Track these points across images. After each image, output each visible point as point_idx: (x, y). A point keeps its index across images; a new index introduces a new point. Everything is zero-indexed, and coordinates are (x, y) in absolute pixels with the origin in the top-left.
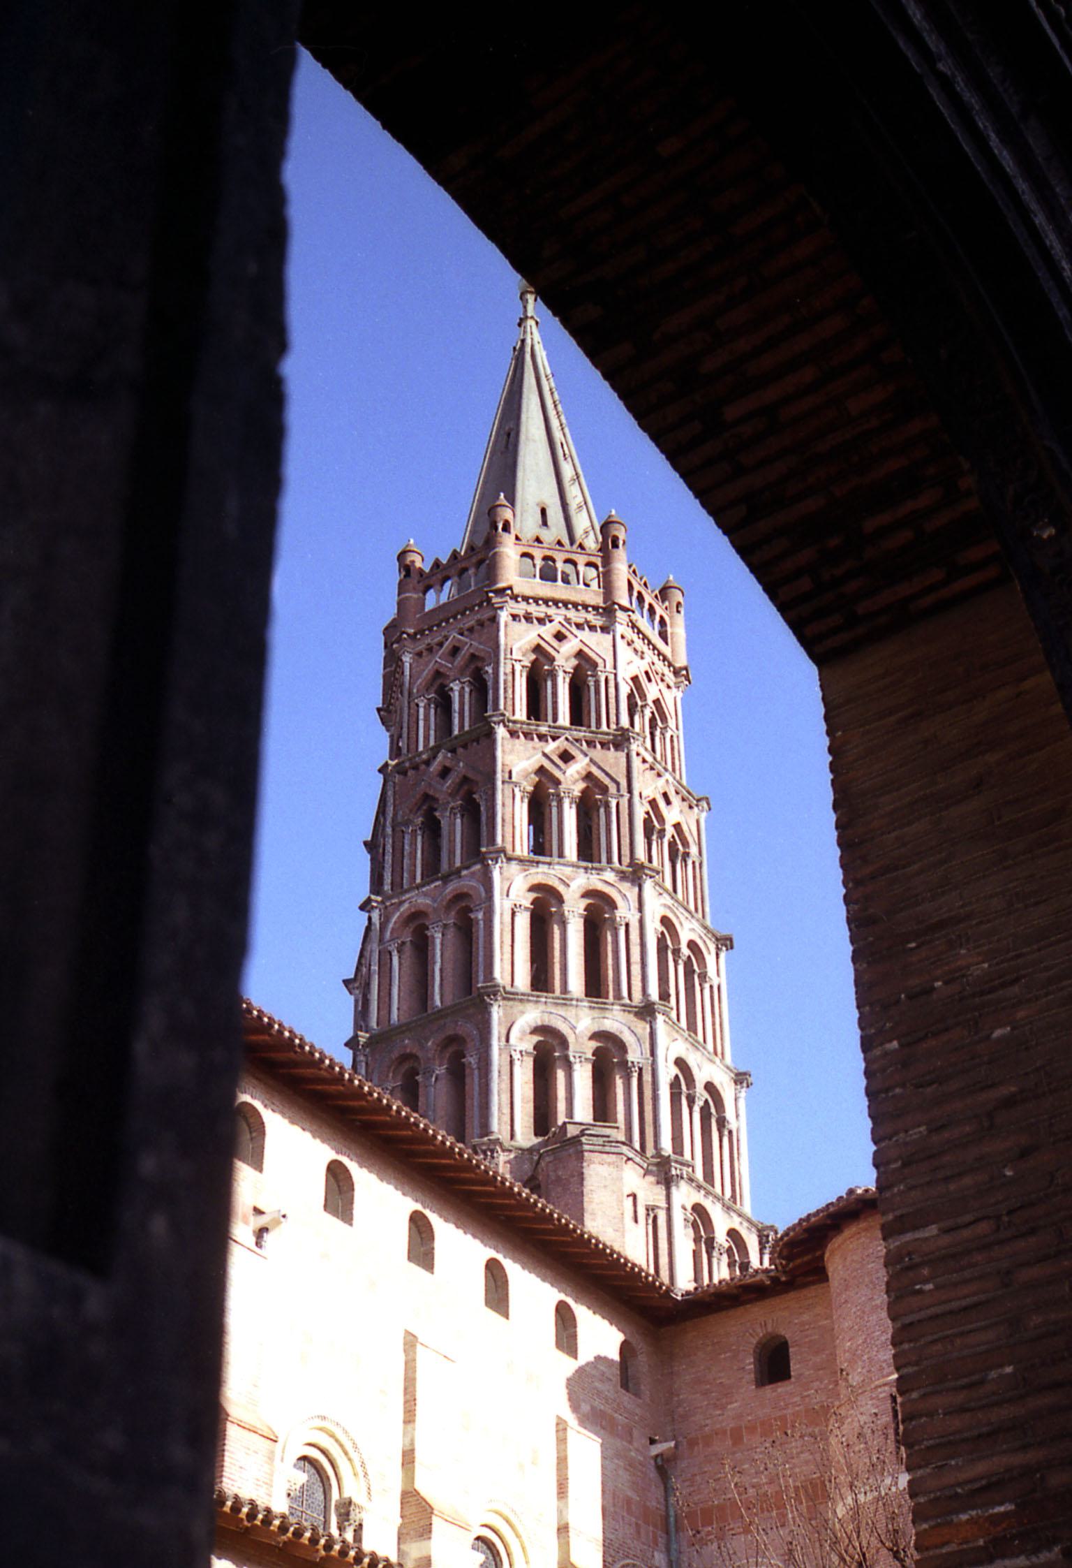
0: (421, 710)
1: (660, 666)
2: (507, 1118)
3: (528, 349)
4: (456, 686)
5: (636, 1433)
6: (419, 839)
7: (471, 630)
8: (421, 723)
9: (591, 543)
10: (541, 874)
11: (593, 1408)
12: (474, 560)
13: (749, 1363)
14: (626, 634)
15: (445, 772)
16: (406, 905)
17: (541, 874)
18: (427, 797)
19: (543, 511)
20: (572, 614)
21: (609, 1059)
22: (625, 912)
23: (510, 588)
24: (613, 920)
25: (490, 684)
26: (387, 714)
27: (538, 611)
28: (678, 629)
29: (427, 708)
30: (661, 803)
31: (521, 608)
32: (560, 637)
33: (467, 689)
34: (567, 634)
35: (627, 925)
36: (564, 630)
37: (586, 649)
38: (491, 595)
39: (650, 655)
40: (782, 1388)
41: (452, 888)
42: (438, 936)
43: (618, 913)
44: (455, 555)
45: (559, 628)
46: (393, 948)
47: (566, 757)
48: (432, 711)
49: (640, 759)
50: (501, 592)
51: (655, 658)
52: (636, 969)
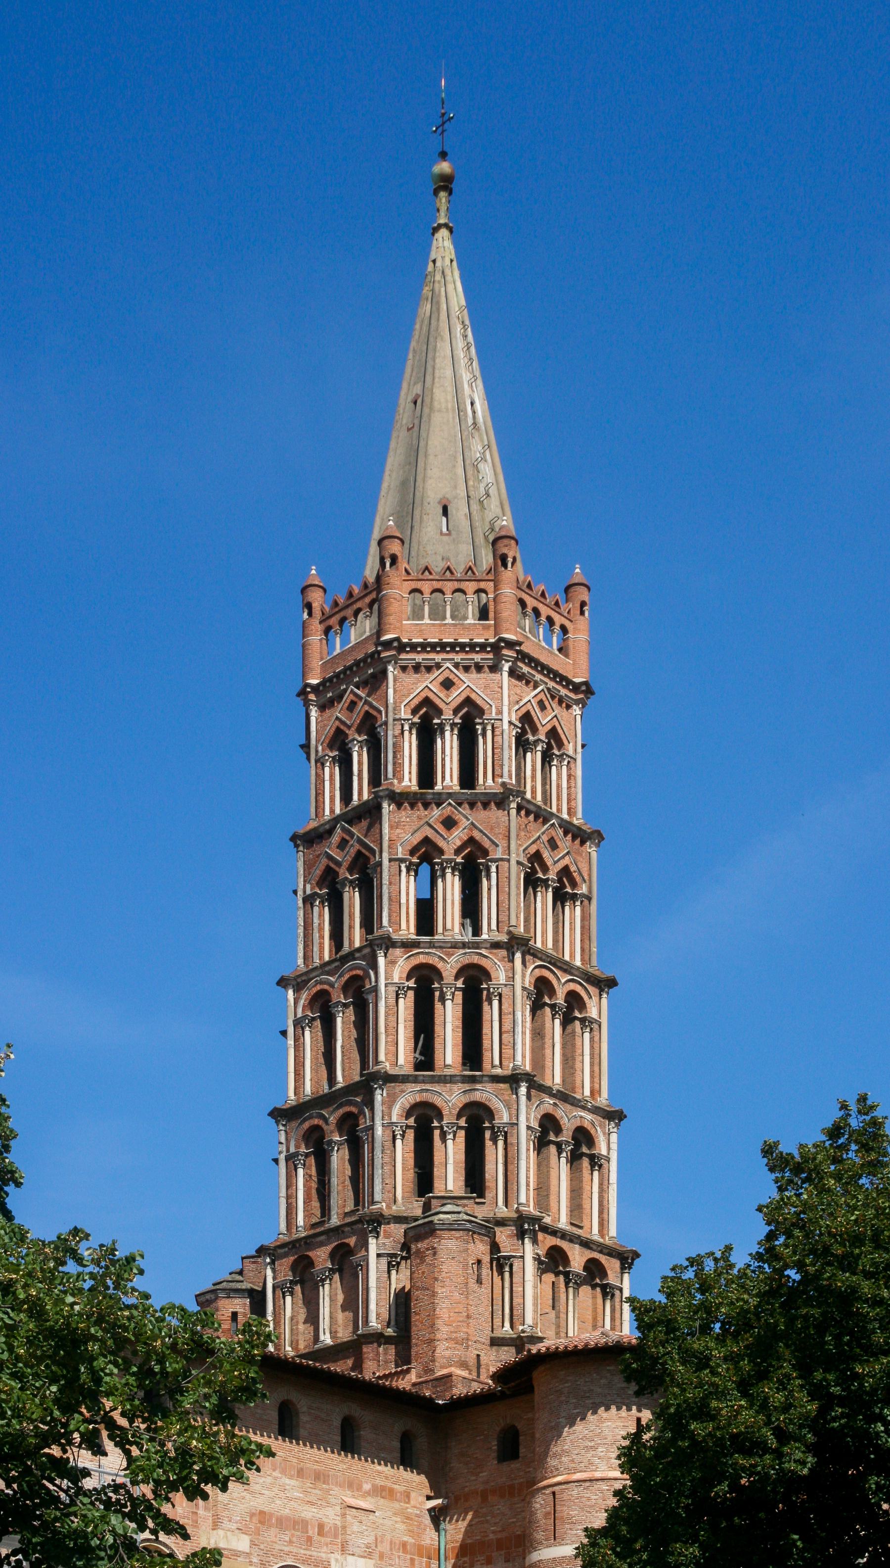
5: (413, 1495)
11: (373, 1485)
12: (367, 600)
28: (580, 635)
32: (448, 684)
34: (455, 680)
36: (452, 677)
40: (515, 1465)
45: (447, 674)
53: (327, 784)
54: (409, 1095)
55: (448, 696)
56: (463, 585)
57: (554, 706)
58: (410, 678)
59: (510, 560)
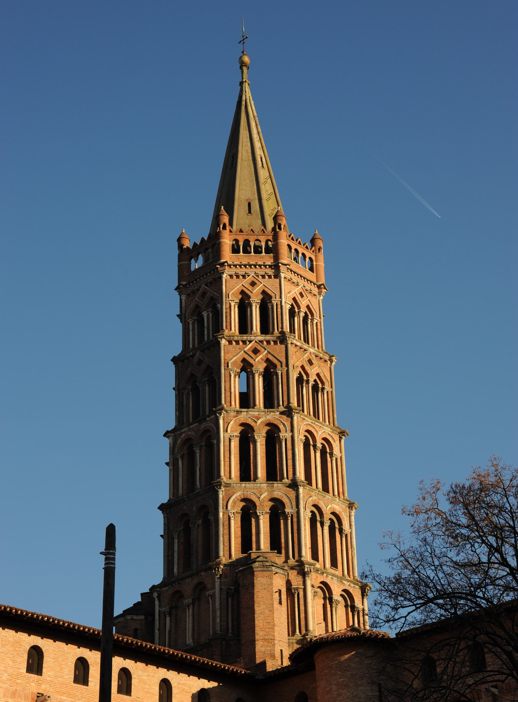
0: (191, 326)
1: (309, 286)
2: (227, 548)
3: (244, 103)
4: (205, 314)
6: (191, 396)
7: (211, 283)
8: (191, 333)
10: (246, 416)
14: (287, 276)
15: (200, 362)
16: (183, 435)
19: (249, 204)
22: (285, 434)
23: (226, 262)
24: (279, 436)
27: (241, 271)
29: (193, 324)
30: (307, 367)
31: (232, 271)
32: (253, 284)
33: (211, 315)
34: (257, 282)
35: (286, 440)
36: (255, 280)
37: (266, 290)
38: (218, 266)
39: (302, 282)
42: (198, 451)
43: (281, 435)
44: (203, 239)
46: (179, 456)
48: (196, 325)
49: (294, 346)
50: (222, 265)
51: (306, 283)
53: (191, 333)
54: (237, 495)
55: (253, 290)
56: (260, 238)
57: (308, 295)
59: (282, 226)
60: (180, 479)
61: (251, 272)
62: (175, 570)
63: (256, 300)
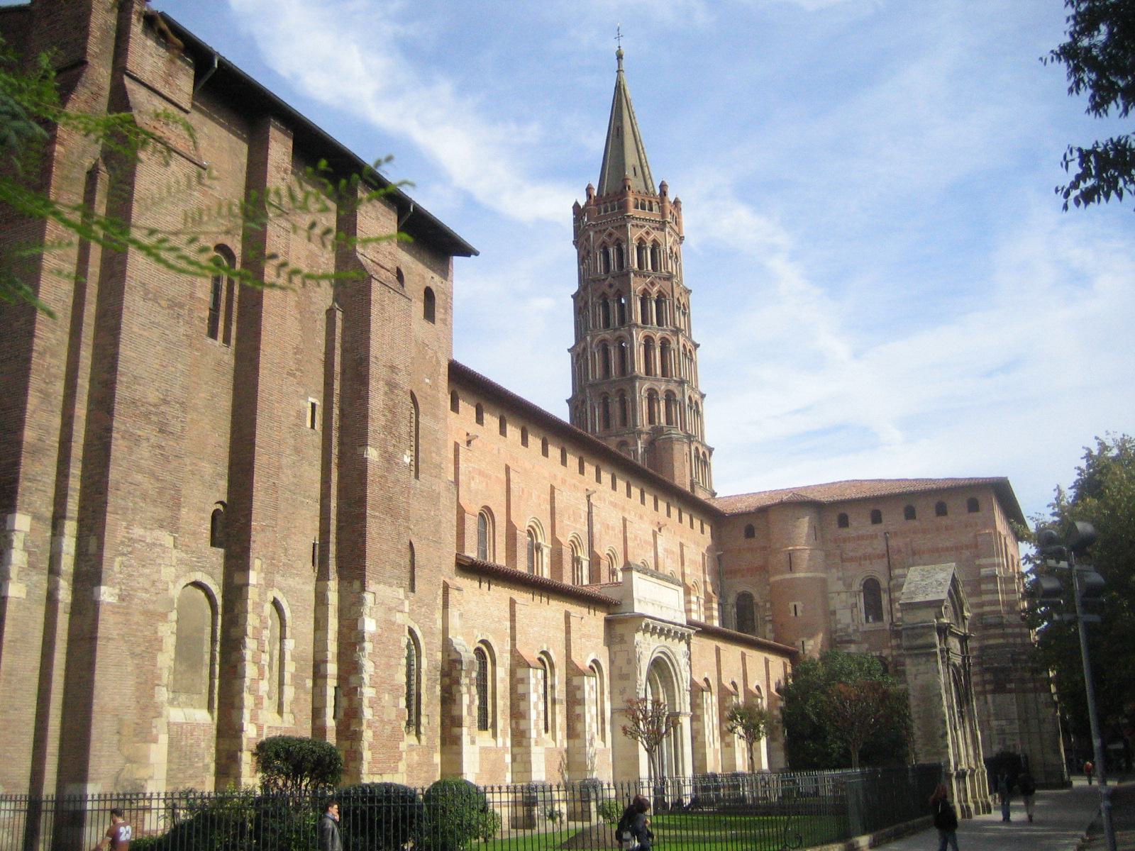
4: (611, 250)
9: (658, 192)
10: (647, 332)
13: (743, 531)
15: (611, 286)
16: (599, 337)
17: (647, 332)
18: (604, 293)
20: (651, 224)
21: (670, 397)
22: (673, 345)
25: (625, 251)
26: (576, 243)
31: (635, 222)
40: (752, 540)
41: (618, 333)
43: (671, 346)
47: (653, 284)
50: (629, 216)
52: (677, 366)
54: (647, 385)
58: (635, 229)
60: (597, 367)
61: (647, 225)
62: (597, 429)
63: (649, 245)
